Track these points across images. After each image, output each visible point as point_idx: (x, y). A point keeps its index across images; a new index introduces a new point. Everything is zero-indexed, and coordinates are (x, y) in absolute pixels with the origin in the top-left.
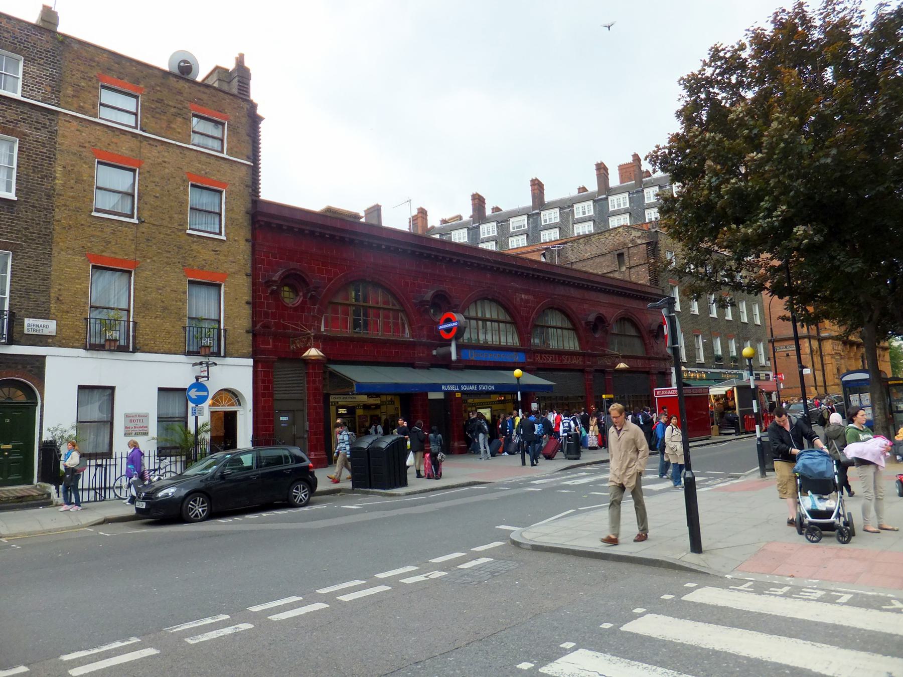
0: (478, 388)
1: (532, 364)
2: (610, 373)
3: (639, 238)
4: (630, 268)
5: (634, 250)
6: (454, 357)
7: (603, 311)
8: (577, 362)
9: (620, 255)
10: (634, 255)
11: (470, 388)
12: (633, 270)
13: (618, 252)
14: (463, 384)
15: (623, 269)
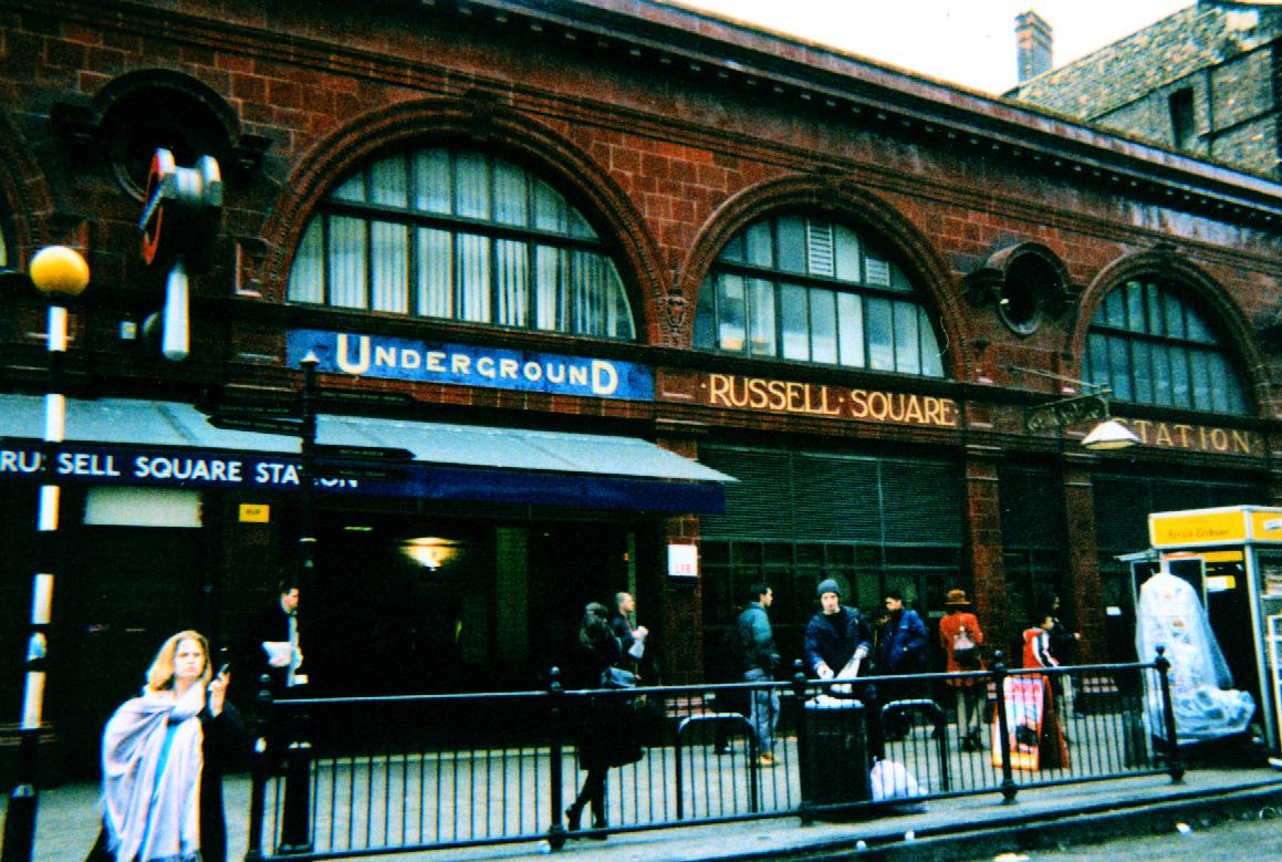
0: (244, 472)
1: (688, 409)
2: (1081, 467)
3: (1251, 32)
4: (1211, 137)
5: (1229, 76)
6: (176, 338)
7: (1048, 237)
8: (936, 413)
9: (1181, 103)
10: (1228, 90)
11: (200, 470)
12: (1222, 142)
13: (1173, 89)
14: (153, 451)
15: (1193, 144)
